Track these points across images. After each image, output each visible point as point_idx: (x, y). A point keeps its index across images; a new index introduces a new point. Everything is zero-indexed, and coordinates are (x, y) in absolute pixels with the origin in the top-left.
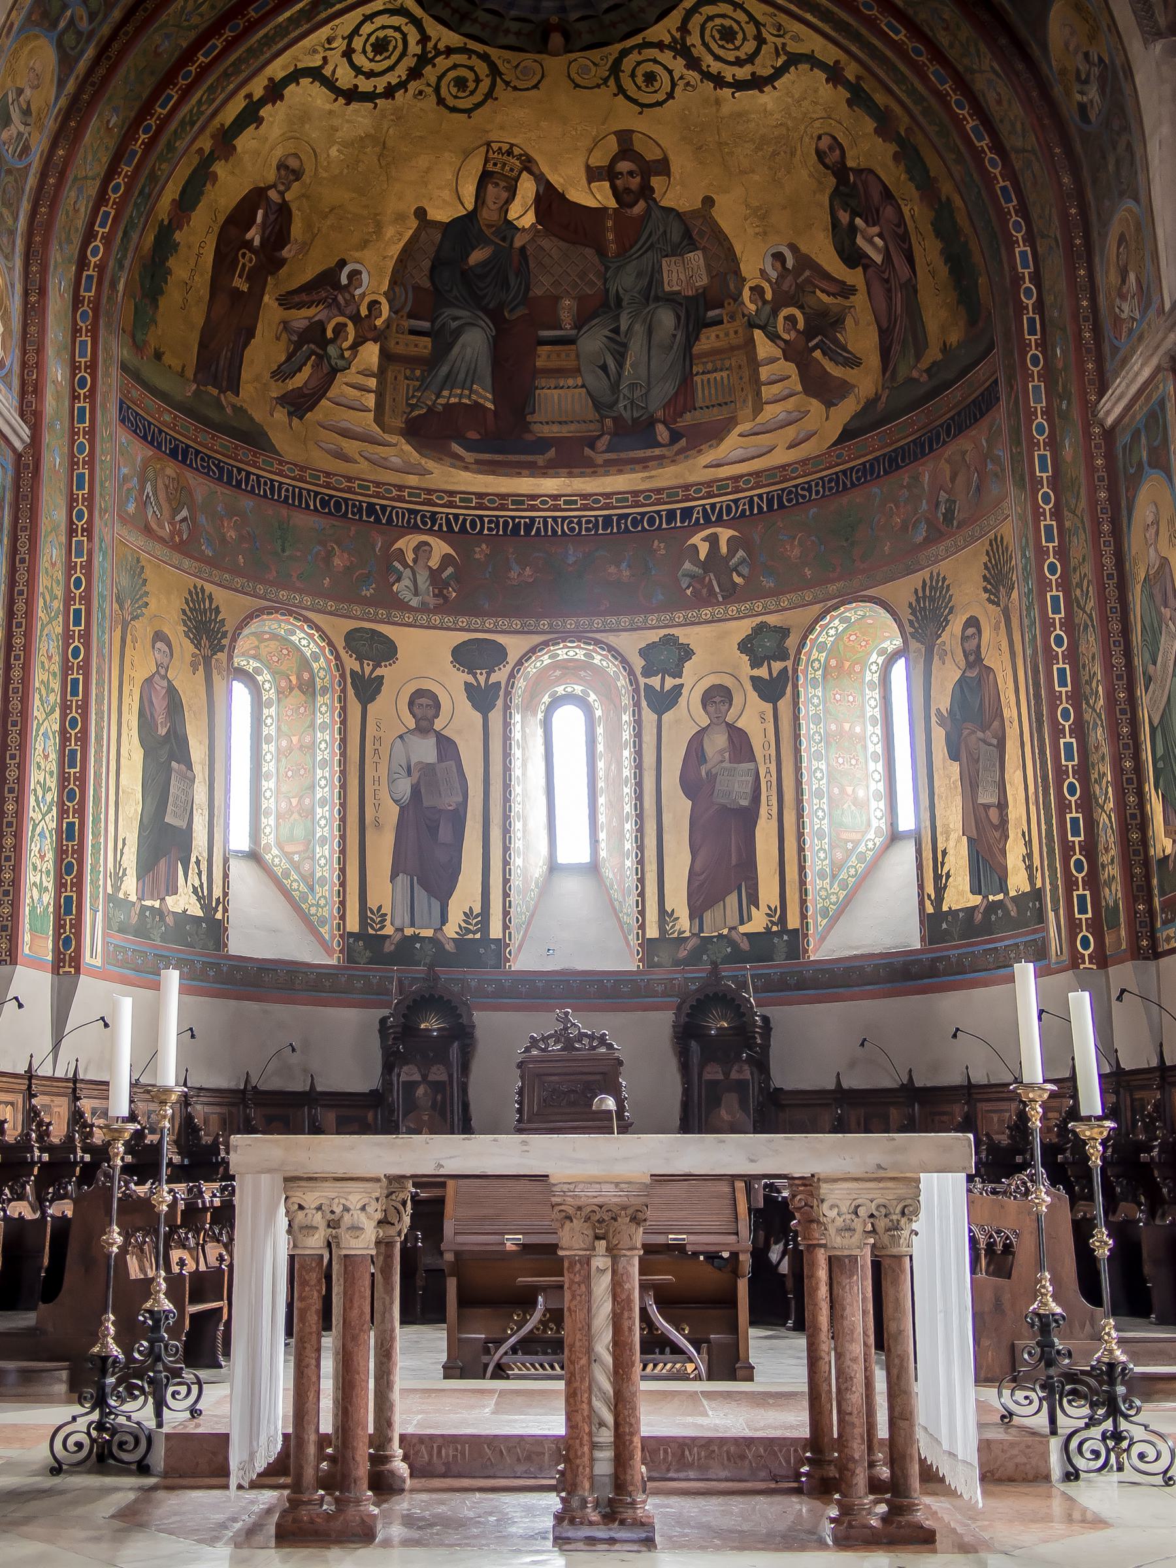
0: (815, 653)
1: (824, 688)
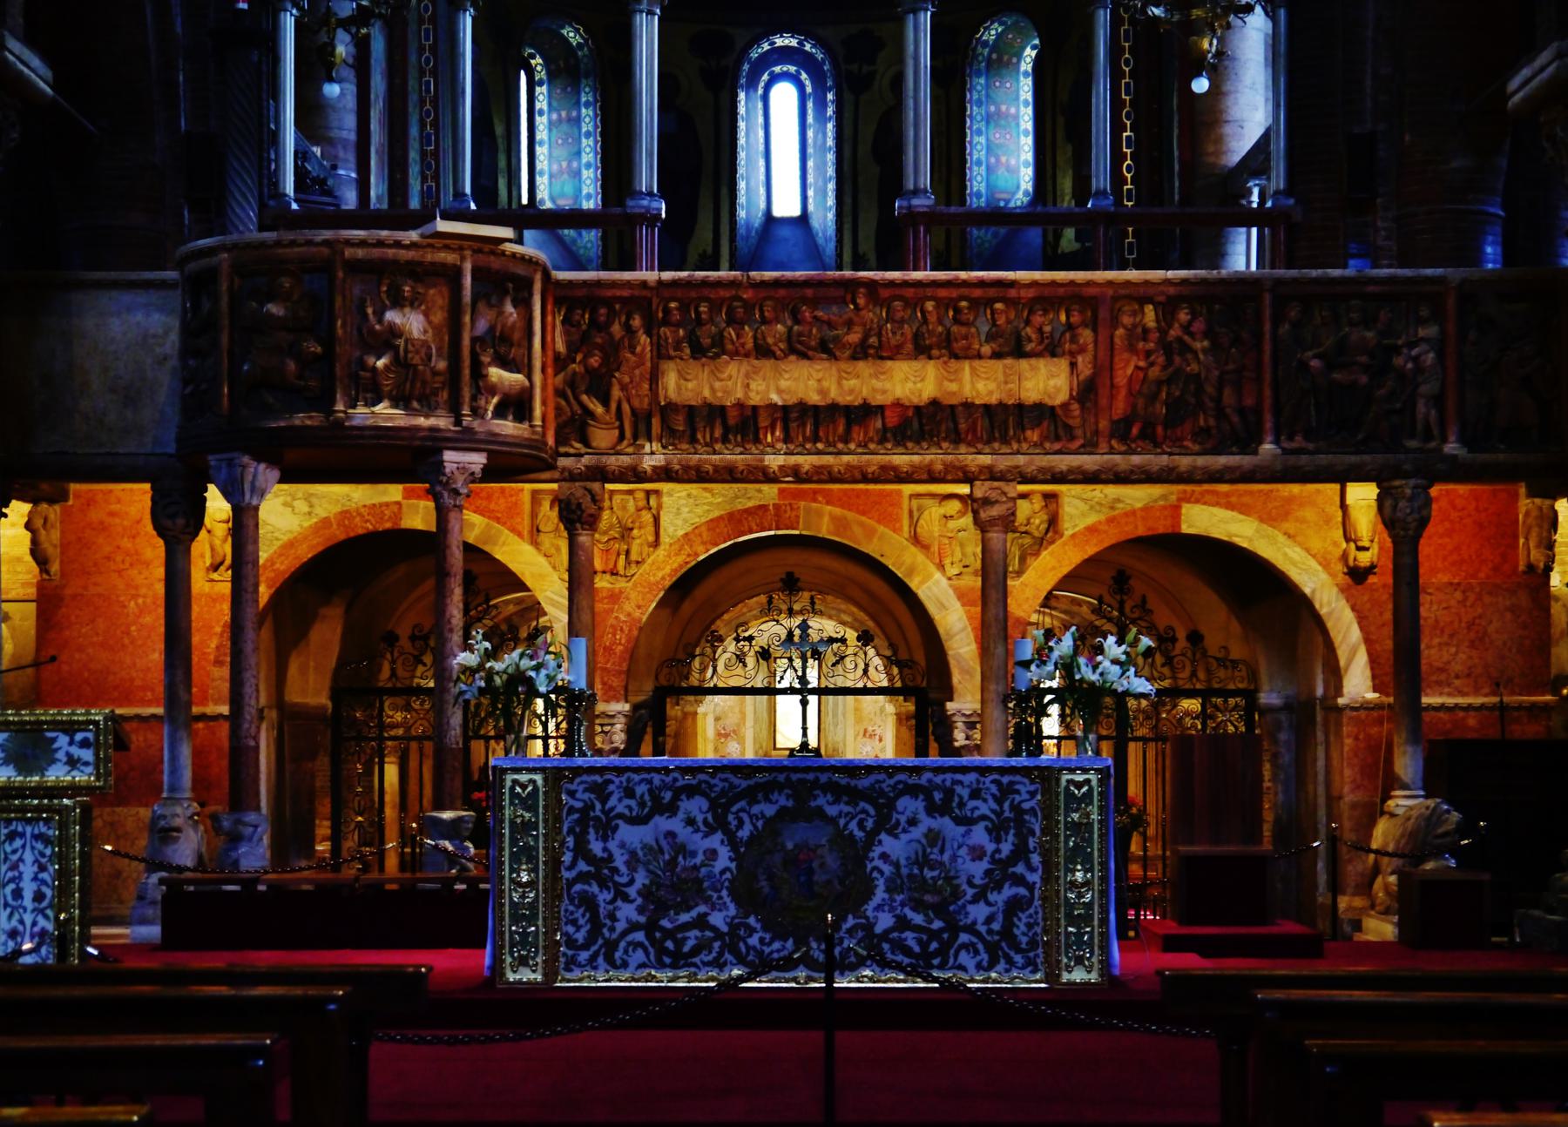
0: (979, 49)
1: (987, 80)
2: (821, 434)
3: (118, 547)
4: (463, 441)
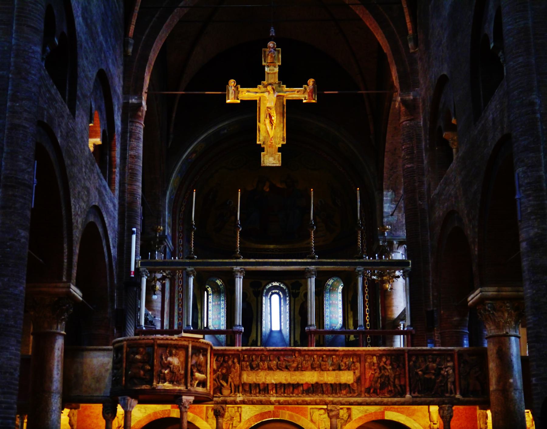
0: (327, 286)
1: (329, 294)
2: (286, 391)
3: (93, 422)
4: (186, 393)
